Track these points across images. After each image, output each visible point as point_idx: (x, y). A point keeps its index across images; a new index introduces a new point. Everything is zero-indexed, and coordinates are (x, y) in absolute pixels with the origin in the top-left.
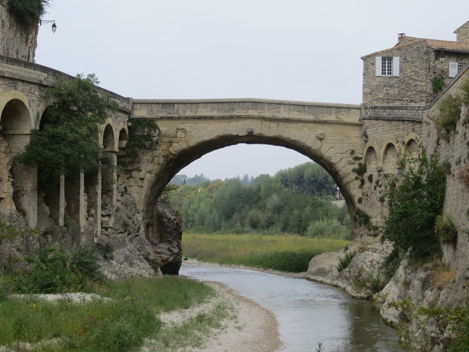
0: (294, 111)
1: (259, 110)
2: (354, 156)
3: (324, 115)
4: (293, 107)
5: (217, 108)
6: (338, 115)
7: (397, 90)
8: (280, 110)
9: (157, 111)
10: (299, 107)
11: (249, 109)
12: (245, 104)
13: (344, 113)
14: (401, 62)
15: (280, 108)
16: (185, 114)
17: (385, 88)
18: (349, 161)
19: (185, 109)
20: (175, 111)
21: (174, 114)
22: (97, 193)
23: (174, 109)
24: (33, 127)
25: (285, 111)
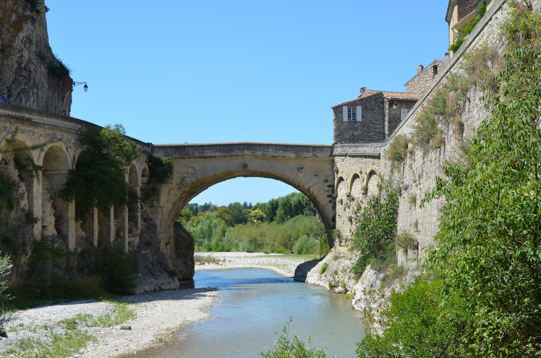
4: (279, 147)
7: (361, 132)
11: (244, 150)
13: (319, 151)
14: (362, 110)
15: (268, 148)
16: (194, 155)
17: (351, 130)
22: (124, 220)
23: (185, 151)
24: (71, 168)
25: (272, 151)
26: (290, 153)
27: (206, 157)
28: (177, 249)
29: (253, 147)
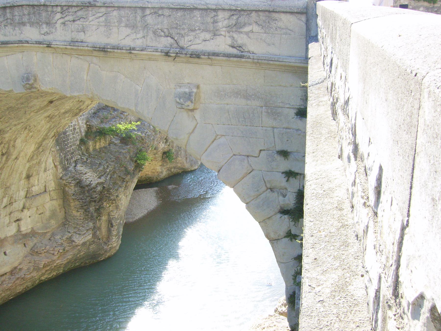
4: (115, 13)
6: (235, 36)
8: (87, 23)
11: (24, 24)
12: (17, 12)
29: (44, 14)
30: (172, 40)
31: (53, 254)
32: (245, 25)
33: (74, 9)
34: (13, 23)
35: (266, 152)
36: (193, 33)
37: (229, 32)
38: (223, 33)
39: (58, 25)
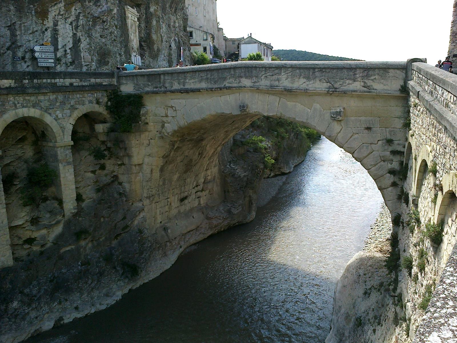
0: (299, 78)
1: (254, 78)
2: (391, 149)
3: (343, 83)
4: (298, 71)
5: (205, 77)
8: (281, 76)
9: (143, 84)
10: (307, 72)
11: (241, 77)
13: (377, 77)
15: (280, 74)
16: (172, 87)
18: (383, 157)
19: (172, 81)
20: (162, 85)
21: (161, 88)
23: (160, 82)
26: (318, 82)
27: (187, 91)
28: (225, 191)
29: (254, 72)
30: (330, 84)
31: (220, 219)
32: (371, 75)
33: (273, 69)
34: (233, 76)
35: (381, 141)
36: (342, 81)
37: (362, 79)
38: (359, 80)
39: (263, 77)
